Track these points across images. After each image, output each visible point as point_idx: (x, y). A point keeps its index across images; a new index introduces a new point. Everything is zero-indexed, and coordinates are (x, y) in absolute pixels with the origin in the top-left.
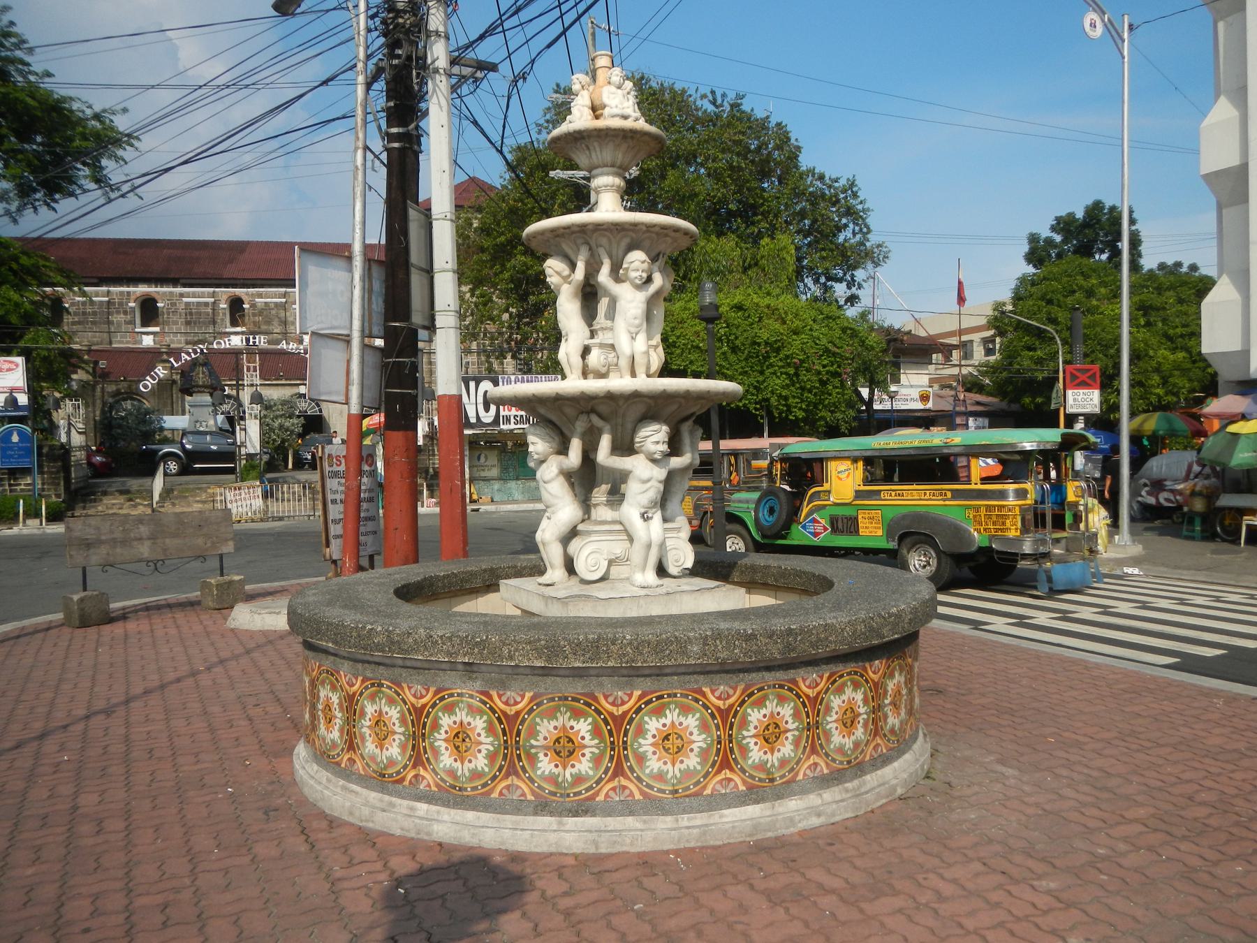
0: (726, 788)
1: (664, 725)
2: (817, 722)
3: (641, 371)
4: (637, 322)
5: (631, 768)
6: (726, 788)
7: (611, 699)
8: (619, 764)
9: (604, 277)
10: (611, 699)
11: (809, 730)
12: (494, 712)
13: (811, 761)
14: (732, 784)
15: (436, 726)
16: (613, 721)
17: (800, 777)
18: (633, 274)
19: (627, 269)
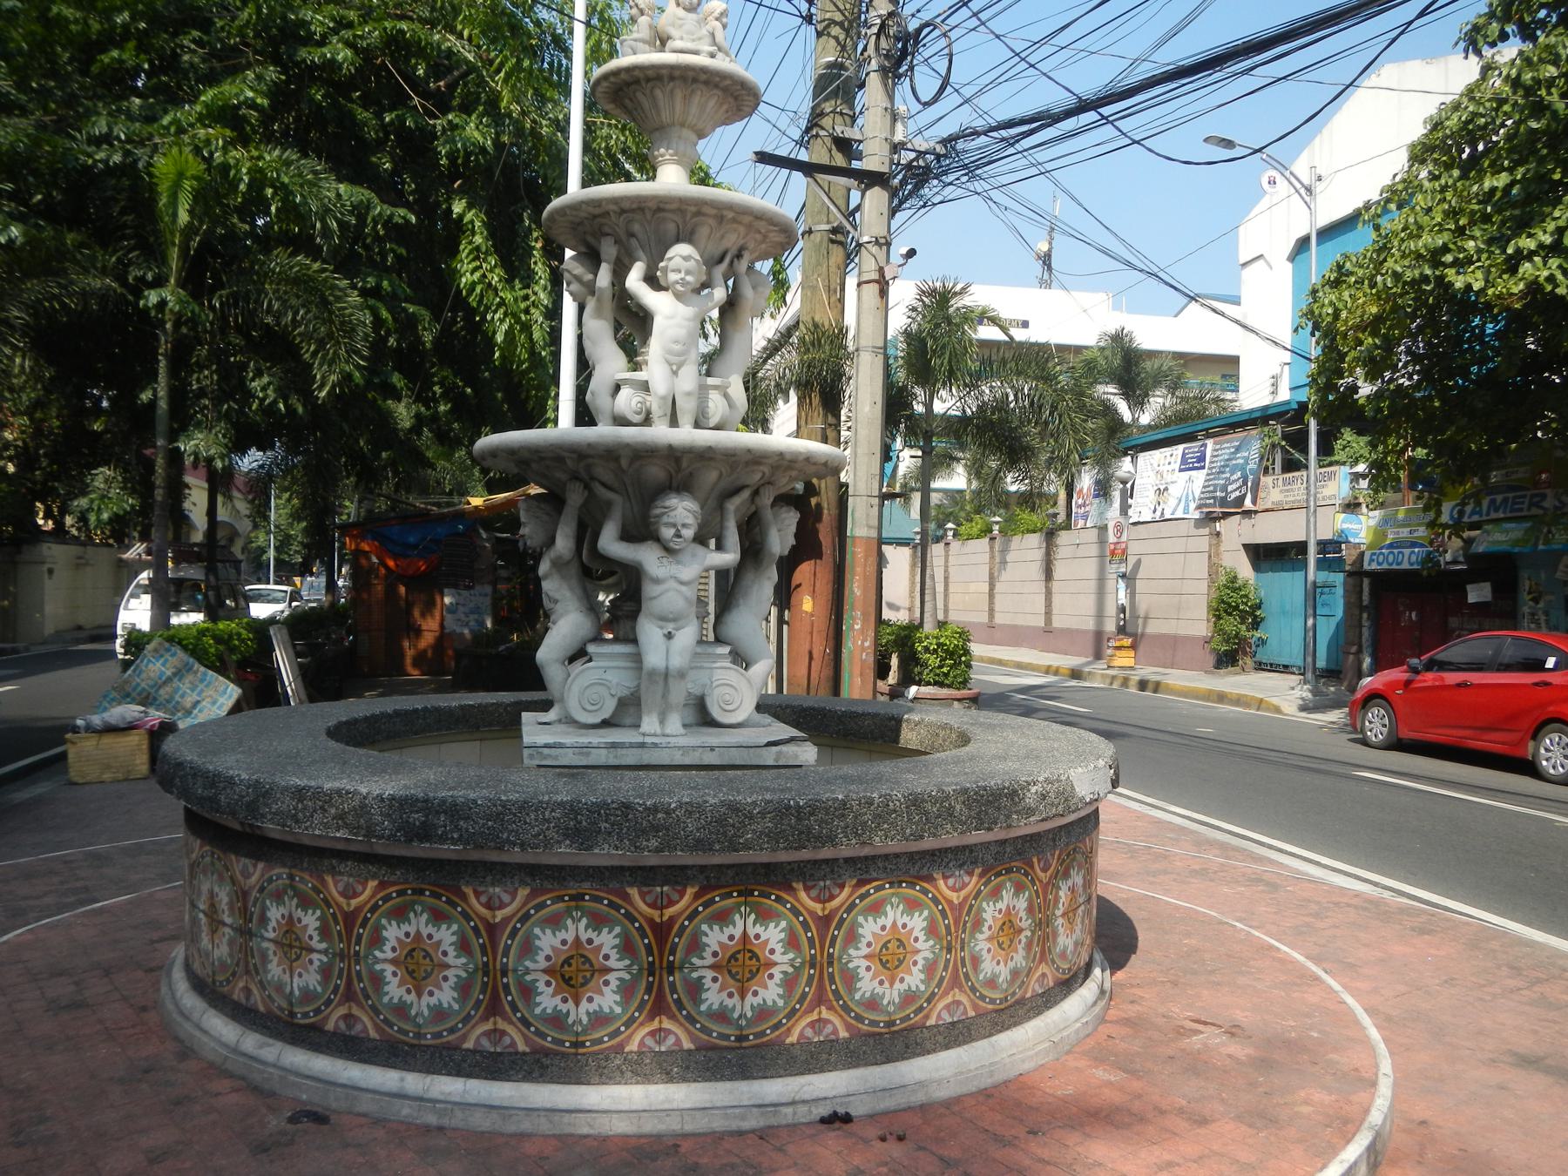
0: (659, 1043)
1: (564, 942)
2: (830, 956)
3: (686, 419)
4: (677, 347)
5: (513, 1005)
6: (659, 1043)
7: (484, 899)
8: (495, 999)
9: (634, 280)
10: (484, 899)
11: (812, 966)
12: (329, 906)
13: (815, 1016)
14: (671, 1040)
15: (264, 920)
16: (487, 931)
17: (793, 1038)
18: (673, 277)
19: (665, 270)
